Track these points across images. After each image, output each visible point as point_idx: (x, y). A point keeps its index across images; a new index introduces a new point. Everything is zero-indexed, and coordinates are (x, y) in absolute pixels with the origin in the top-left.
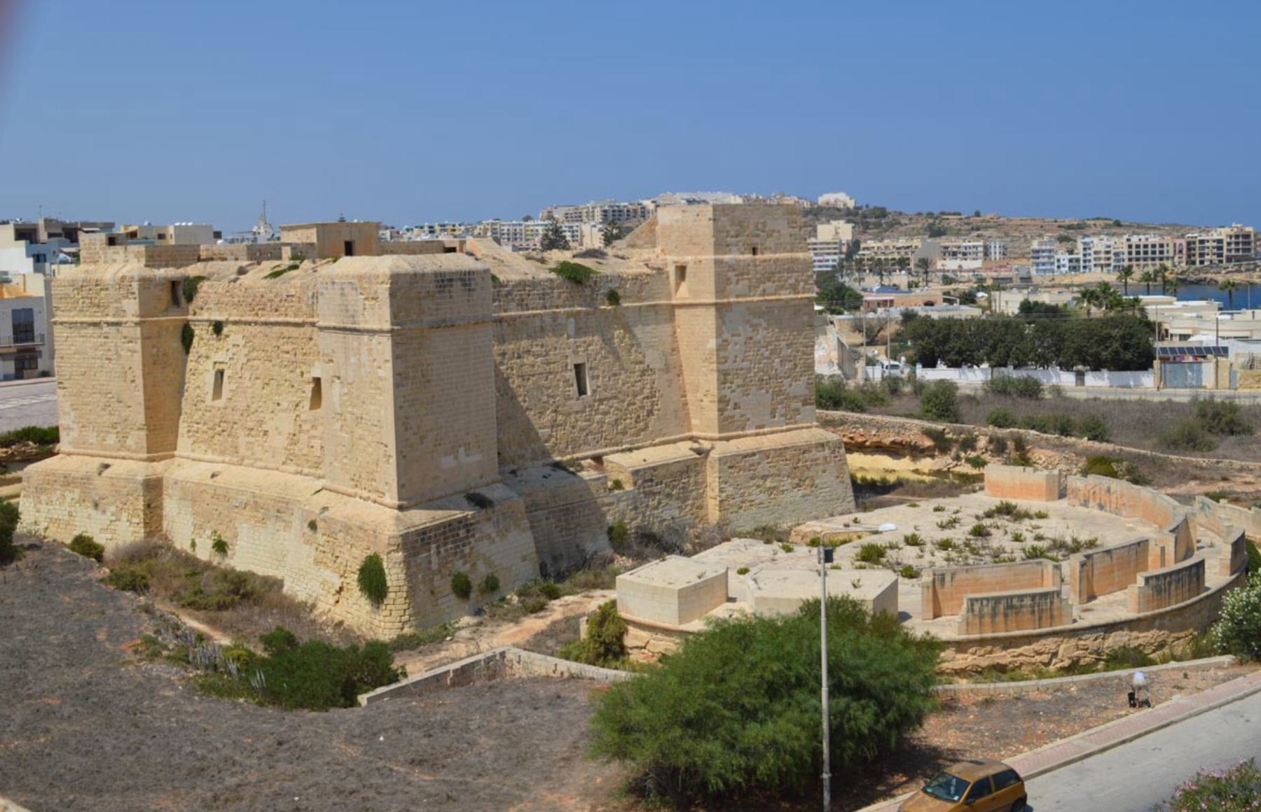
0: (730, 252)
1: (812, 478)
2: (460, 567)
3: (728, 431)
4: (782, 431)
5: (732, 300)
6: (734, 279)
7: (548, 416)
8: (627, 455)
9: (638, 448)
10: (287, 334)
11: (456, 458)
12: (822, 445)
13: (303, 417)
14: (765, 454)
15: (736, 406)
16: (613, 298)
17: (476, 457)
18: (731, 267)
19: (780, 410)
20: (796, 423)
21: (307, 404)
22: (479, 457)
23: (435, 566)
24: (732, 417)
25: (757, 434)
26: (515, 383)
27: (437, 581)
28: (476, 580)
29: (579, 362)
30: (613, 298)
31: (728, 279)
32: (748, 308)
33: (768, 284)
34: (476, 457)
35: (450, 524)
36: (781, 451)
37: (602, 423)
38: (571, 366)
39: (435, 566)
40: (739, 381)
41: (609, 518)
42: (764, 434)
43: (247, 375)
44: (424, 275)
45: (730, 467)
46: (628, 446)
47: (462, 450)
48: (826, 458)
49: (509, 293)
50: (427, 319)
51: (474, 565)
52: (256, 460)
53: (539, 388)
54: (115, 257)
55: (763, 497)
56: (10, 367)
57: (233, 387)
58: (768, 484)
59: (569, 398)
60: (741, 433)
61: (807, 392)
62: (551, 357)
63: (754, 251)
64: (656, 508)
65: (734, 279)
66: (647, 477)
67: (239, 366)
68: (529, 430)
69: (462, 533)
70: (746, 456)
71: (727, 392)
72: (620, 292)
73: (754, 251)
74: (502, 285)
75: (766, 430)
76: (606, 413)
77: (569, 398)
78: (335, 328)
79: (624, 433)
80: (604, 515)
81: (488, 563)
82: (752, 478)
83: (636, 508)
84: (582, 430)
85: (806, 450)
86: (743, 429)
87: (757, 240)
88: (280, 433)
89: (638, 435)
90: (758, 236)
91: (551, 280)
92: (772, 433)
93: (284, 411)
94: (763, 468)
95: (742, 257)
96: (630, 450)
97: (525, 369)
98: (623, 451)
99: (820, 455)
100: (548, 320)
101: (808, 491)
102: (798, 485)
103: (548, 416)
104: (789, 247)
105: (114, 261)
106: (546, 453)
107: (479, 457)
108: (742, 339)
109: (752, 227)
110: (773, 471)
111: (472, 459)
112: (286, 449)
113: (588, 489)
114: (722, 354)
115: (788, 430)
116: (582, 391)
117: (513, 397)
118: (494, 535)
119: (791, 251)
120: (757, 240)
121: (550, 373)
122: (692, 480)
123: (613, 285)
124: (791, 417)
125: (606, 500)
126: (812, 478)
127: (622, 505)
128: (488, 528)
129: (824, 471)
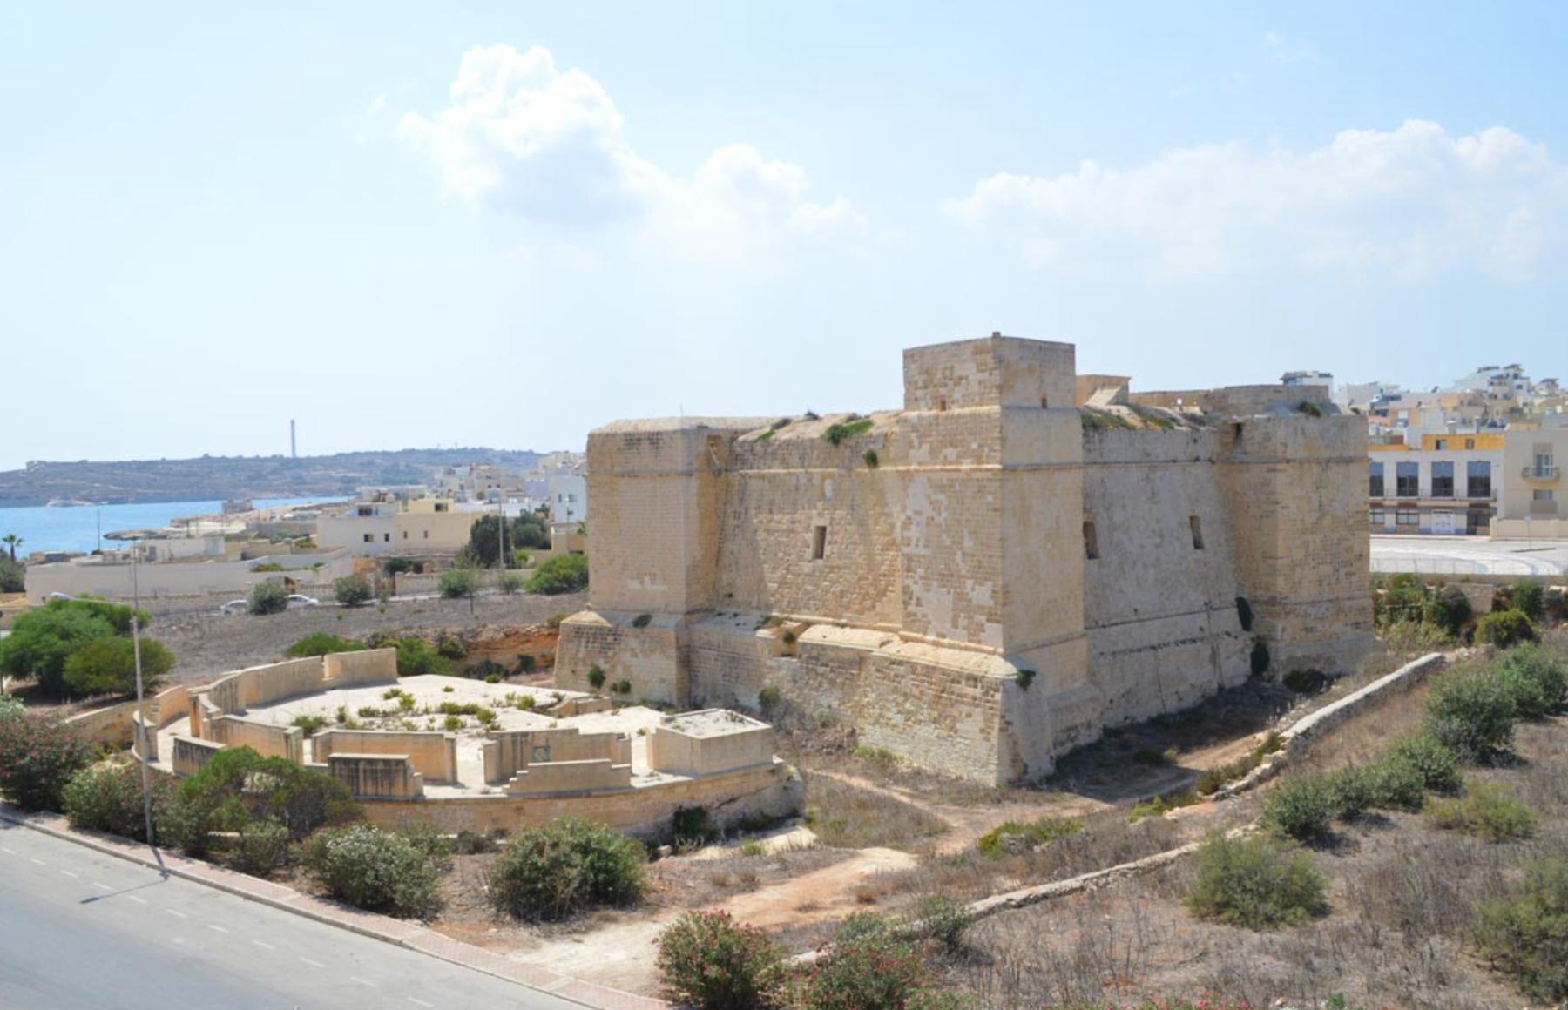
0: (918, 408)
1: (954, 719)
2: (603, 666)
3: (910, 630)
4: (961, 648)
5: (912, 468)
6: (916, 442)
7: (781, 572)
8: (838, 629)
9: (854, 627)
12: (974, 679)
14: (912, 666)
15: (919, 604)
16: (872, 460)
17: (661, 588)
18: (915, 429)
19: (963, 621)
20: (979, 642)
22: (665, 588)
23: (581, 655)
25: (936, 644)
26: (761, 535)
27: (580, 668)
28: (610, 680)
29: (822, 523)
30: (872, 460)
31: (911, 442)
32: (929, 480)
33: (951, 452)
34: (661, 588)
35: (601, 628)
36: (930, 670)
37: (827, 592)
38: (812, 528)
39: (581, 655)
40: (921, 571)
41: (767, 682)
42: (943, 646)
44: (614, 435)
45: (878, 670)
46: (843, 621)
47: (647, 579)
48: (975, 698)
49: (774, 453)
50: (617, 469)
51: (613, 667)
53: (779, 543)
55: (899, 719)
56: (1462, 521)
58: (908, 705)
59: (801, 558)
60: (919, 636)
61: (992, 603)
62: (797, 517)
63: (944, 407)
64: (817, 689)
65: (916, 442)
66: (819, 656)
68: (761, 580)
69: (610, 639)
70: (893, 663)
71: (909, 582)
72: (880, 455)
73: (944, 407)
74: (770, 445)
75: (946, 641)
76: (833, 582)
77: (801, 558)
79: (847, 608)
80: (763, 676)
81: (626, 668)
82: (895, 691)
83: (795, 681)
84: (806, 592)
85: (956, 678)
86: (925, 633)
87: (943, 391)
89: (861, 612)
90: (946, 385)
91: (812, 440)
92: (951, 646)
94: (907, 683)
95: (925, 413)
96: (843, 626)
97: (773, 525)
98: (838, 625)
99: (970, 691)
100: (804, 480)
101: (944, 733)
102: (935, 721)
103: (781, 572)
104: (977, 399)
106: (769, 607)
107: (665, 588)
108: (923, 519)
109: (939, 375)
110: (916, 692)
111: (655, 587)
113: (754, 644)
114: (906, 534)
115: (967, 649)
116: (819, 554)
117: (755, 549)
119: (981, 404)
120: (943, 391)
121: (792, 531)
122: (863, 675)
123: (872, 446)
124: (975, 633)
125: (769, 663)
126: (954, 719)
127: (782, 673)
128: (633, 643)
129: (969, 716)
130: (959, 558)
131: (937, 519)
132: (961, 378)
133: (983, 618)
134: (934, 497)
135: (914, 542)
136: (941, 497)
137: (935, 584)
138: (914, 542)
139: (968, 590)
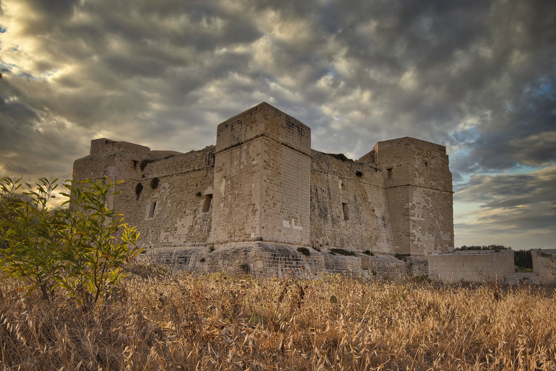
6: (417, 175)
10: (193, 177)
11: (290, 224)
13: (198, 216)
21: (201, 209)
22: (301, 228)
24: (417, 245)
40: (421, 228)
43: (169, 201)
47: (293, 220)
52: (170, 243)
54: (107, 149)
57: (161, 209)
65: (417, 175)
67: (165, 198)
78: (226, 149)
87: (426, 159)
88: (184, 227)
90: (428, 157)
93: (187, 215)
105: (107, 151)
112: (186, 235)
118: (310, 271)
120: (426, 159)
130: (437, 223)
131: (427, 207)
132: (434, 157)
133: (447, 246)
134: (426, 198)
135: (417, 214)
136: (429, 198)
137: (427, 232)
138: (417, 214)
139: (441, 234)
